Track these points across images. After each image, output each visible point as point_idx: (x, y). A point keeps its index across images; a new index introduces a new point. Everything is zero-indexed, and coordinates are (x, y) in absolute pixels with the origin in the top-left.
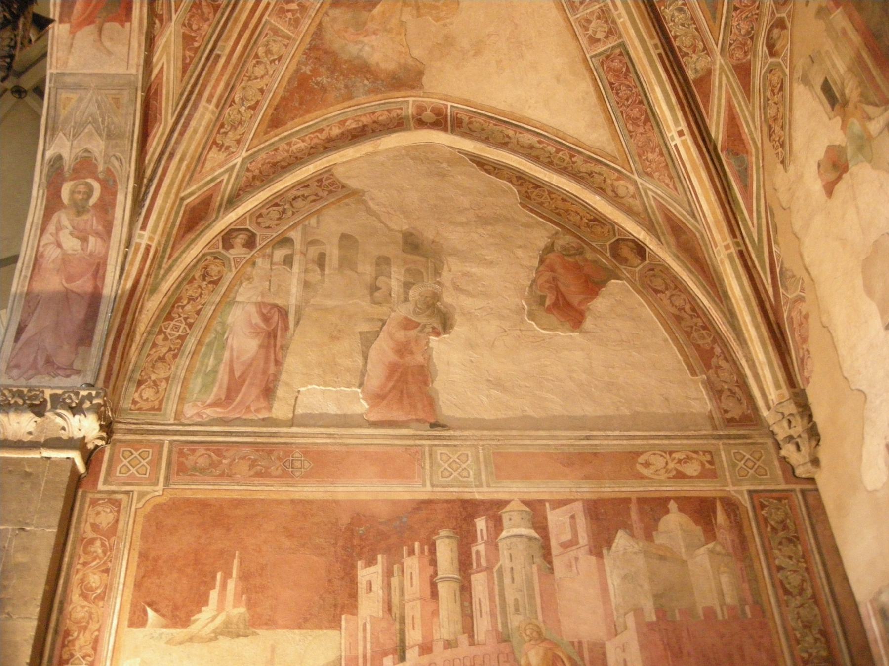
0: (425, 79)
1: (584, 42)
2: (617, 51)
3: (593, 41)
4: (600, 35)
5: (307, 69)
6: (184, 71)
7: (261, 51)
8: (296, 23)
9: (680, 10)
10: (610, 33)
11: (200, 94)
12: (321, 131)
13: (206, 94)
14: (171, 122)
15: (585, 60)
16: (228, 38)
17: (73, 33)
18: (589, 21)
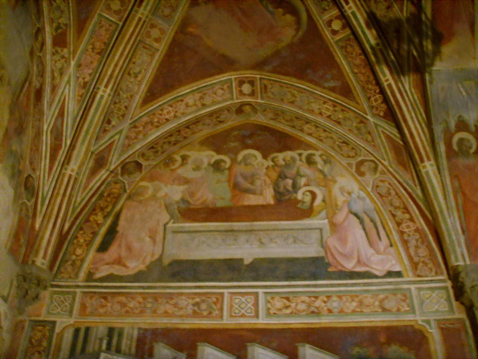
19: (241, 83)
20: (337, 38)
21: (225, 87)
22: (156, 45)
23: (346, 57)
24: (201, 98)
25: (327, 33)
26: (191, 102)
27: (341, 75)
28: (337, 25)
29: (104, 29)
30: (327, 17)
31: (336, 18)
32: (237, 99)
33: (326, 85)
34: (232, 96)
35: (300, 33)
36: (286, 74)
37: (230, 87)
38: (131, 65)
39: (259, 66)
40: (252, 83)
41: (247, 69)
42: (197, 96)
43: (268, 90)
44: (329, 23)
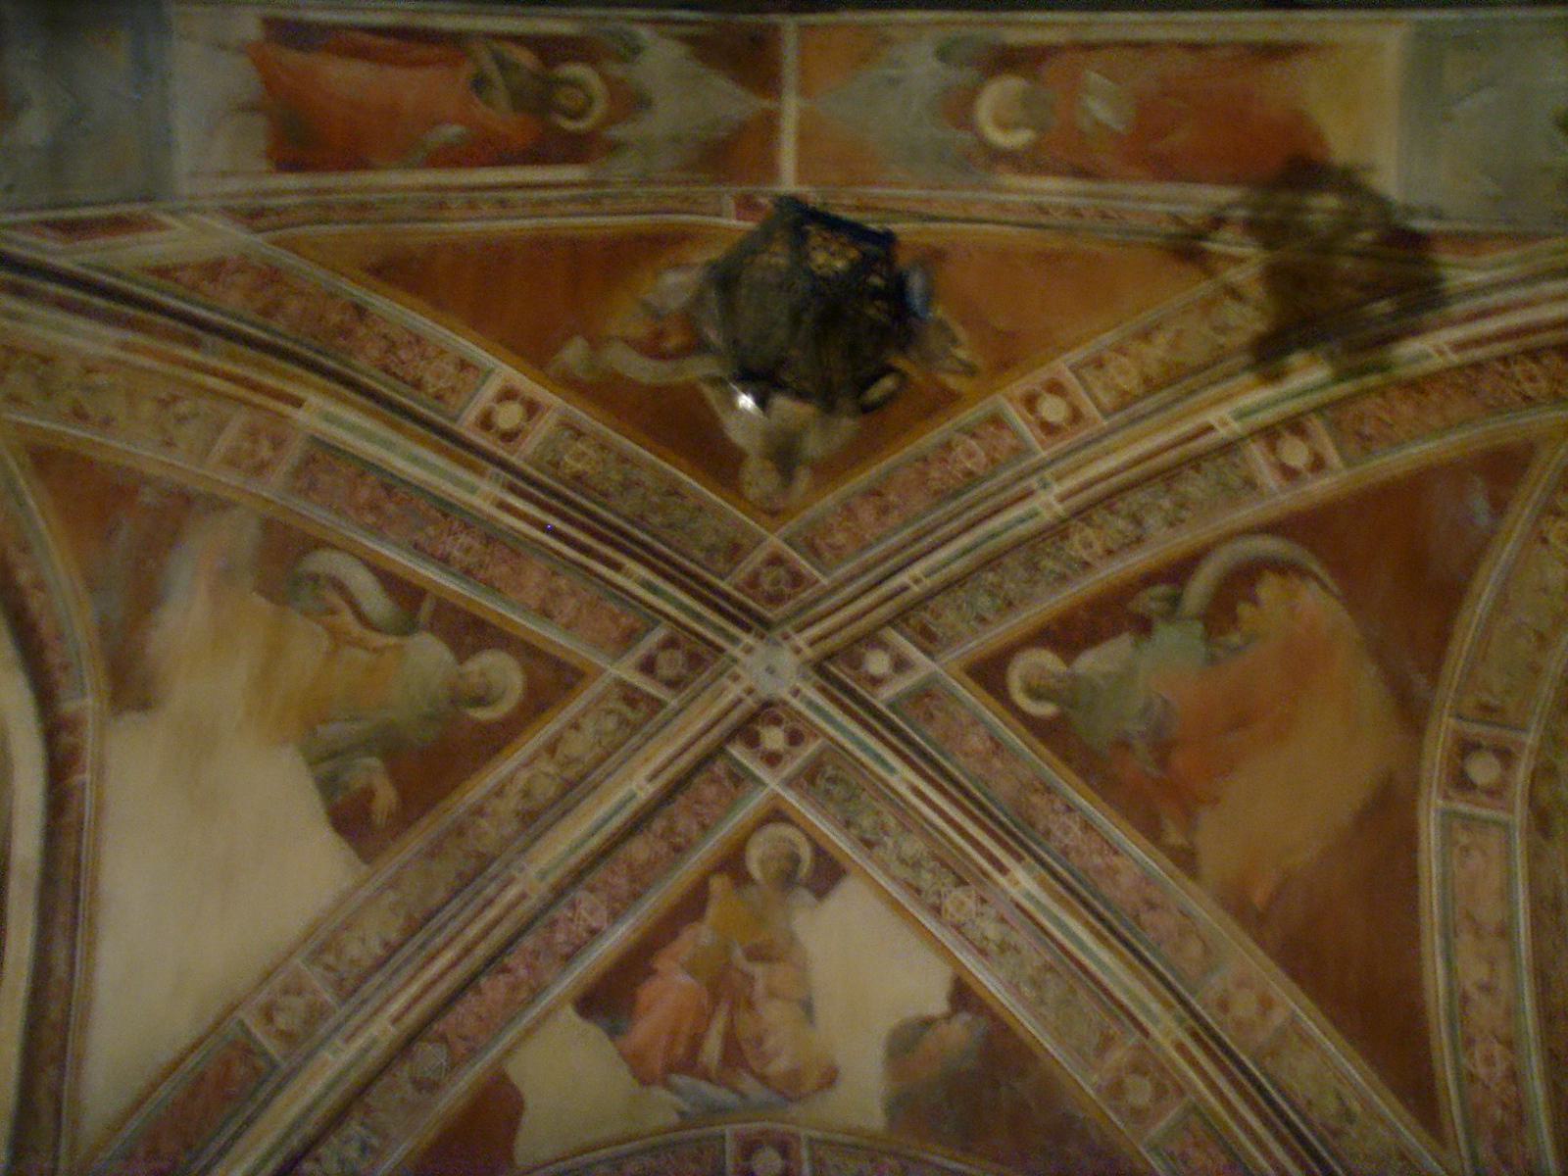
0: (130, 718)
1: (262, 998)
2: (261, 1063)
3: (268, 1014)
4: (282, 1021)
5: (147, 496)
6: (162, 272)
7: (183, 408)
8: (232, 462)
9: (365, 1148)
10: (288, 1037)
11: (130, 324)
12: (25, 549)
13: (131, 337)
14: (64, 263)
15: (233, 1008)
16: (232, 357)
17: (244, 48)
18: (299, 993)
19: (1462, 782)
20: (1333, 457)
21: (1464, 839)
22: (1278, 1017)
23: (1397, 444)
24: (1477, 929)
25: (1320, 488)
26: (1474, 972)
27: (1451, 472)
28: (1296, 454)
29: (1190, 1151)
30: (1269, 479)
31: (1273, 449)
32: (1511, 811)
33: (1483, 520)
34: (1496, 823)
35: (1315, 567)
36: (1443, 638)
37: (1469, 822)
38: (1314, 1116)
39: (1411, 714)
40: (1467, 747)
41: (1415, 754)
42: (1465, 941)
43: (1494, 702)
44: (1289, 473)
